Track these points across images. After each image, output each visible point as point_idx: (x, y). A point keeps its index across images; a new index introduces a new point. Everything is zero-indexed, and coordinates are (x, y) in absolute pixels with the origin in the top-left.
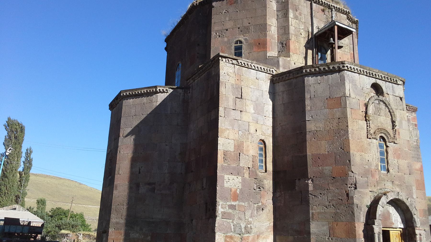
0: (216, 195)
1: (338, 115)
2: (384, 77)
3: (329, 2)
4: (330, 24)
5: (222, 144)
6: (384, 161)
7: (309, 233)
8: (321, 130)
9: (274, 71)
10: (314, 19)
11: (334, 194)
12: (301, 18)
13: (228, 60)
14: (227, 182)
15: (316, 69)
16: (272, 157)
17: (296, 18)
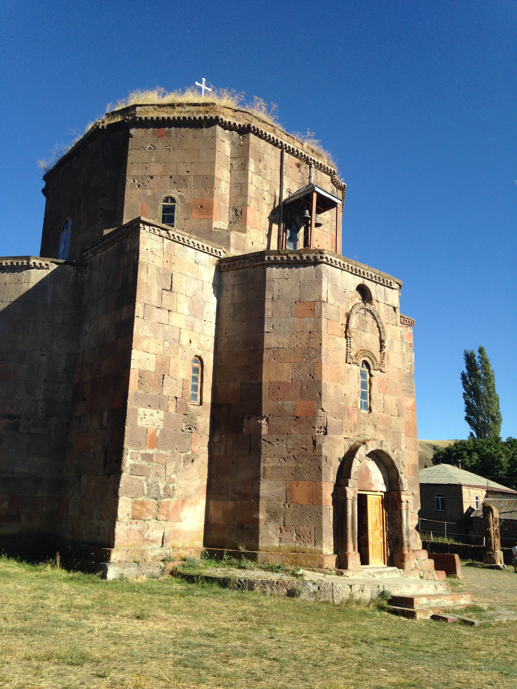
0: (124, 439)
1: (309, 327)
2: (375, 277)
3: (308, 153)
4: (306, 189)
5: (137, 360)
6: (366, 395)
7: (257, 497)
8: (285, 347)
9: (222, 253)
10: (285, 178)
12: (265, 173)
13: (154, 229)
14: (142, 419)
15: (283, 256)
16: (211, 383)
17: (258, 172)
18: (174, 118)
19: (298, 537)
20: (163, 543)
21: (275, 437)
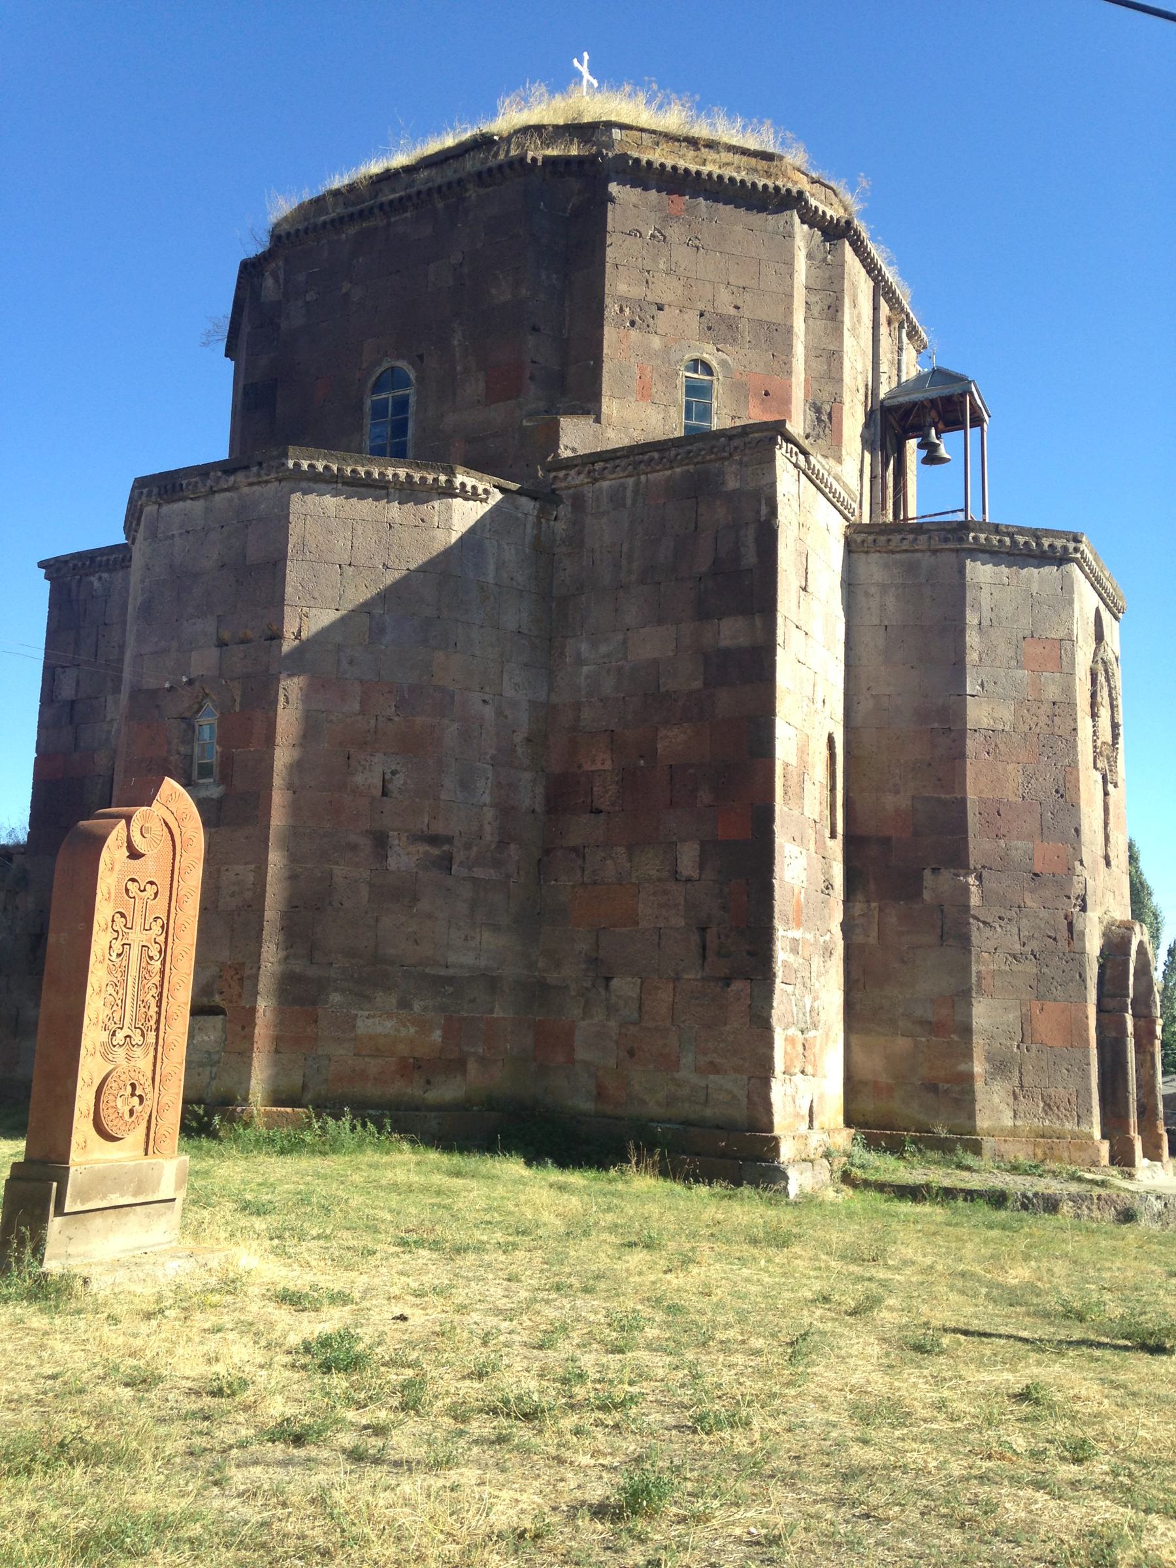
1: (1052, 692)
7: (967, 1031)
8: (1007, 728)
11: (1038, 921)
18: (710, 174)
19: (1046, 1108)
20: (811, 1121)
21: (998, 910)
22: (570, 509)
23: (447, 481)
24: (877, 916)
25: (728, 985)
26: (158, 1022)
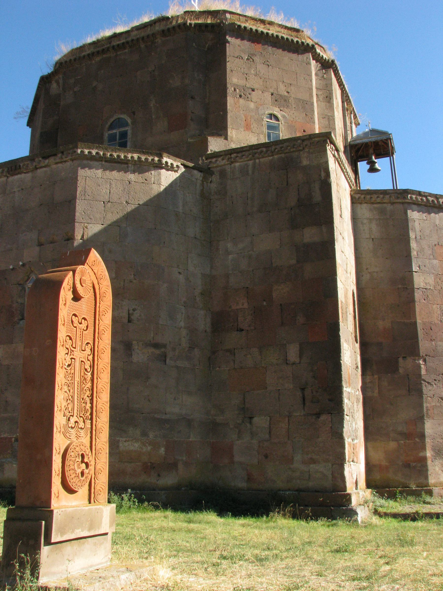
7: (422, 436)
8: (431, 288)
18: (273, 34)
21: (433, 376)
22: (218, 177)
23: (158, 160)
24: (377, 383)
25: (319, 418)
26: (92, 414)
